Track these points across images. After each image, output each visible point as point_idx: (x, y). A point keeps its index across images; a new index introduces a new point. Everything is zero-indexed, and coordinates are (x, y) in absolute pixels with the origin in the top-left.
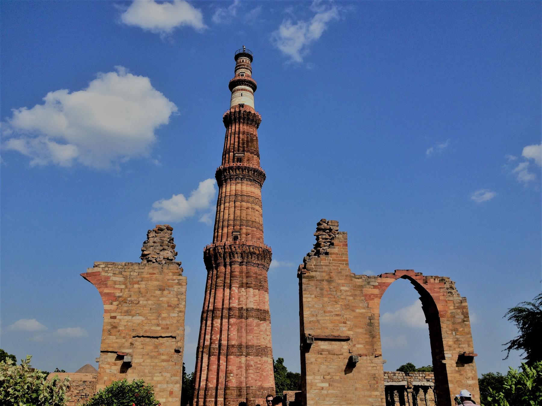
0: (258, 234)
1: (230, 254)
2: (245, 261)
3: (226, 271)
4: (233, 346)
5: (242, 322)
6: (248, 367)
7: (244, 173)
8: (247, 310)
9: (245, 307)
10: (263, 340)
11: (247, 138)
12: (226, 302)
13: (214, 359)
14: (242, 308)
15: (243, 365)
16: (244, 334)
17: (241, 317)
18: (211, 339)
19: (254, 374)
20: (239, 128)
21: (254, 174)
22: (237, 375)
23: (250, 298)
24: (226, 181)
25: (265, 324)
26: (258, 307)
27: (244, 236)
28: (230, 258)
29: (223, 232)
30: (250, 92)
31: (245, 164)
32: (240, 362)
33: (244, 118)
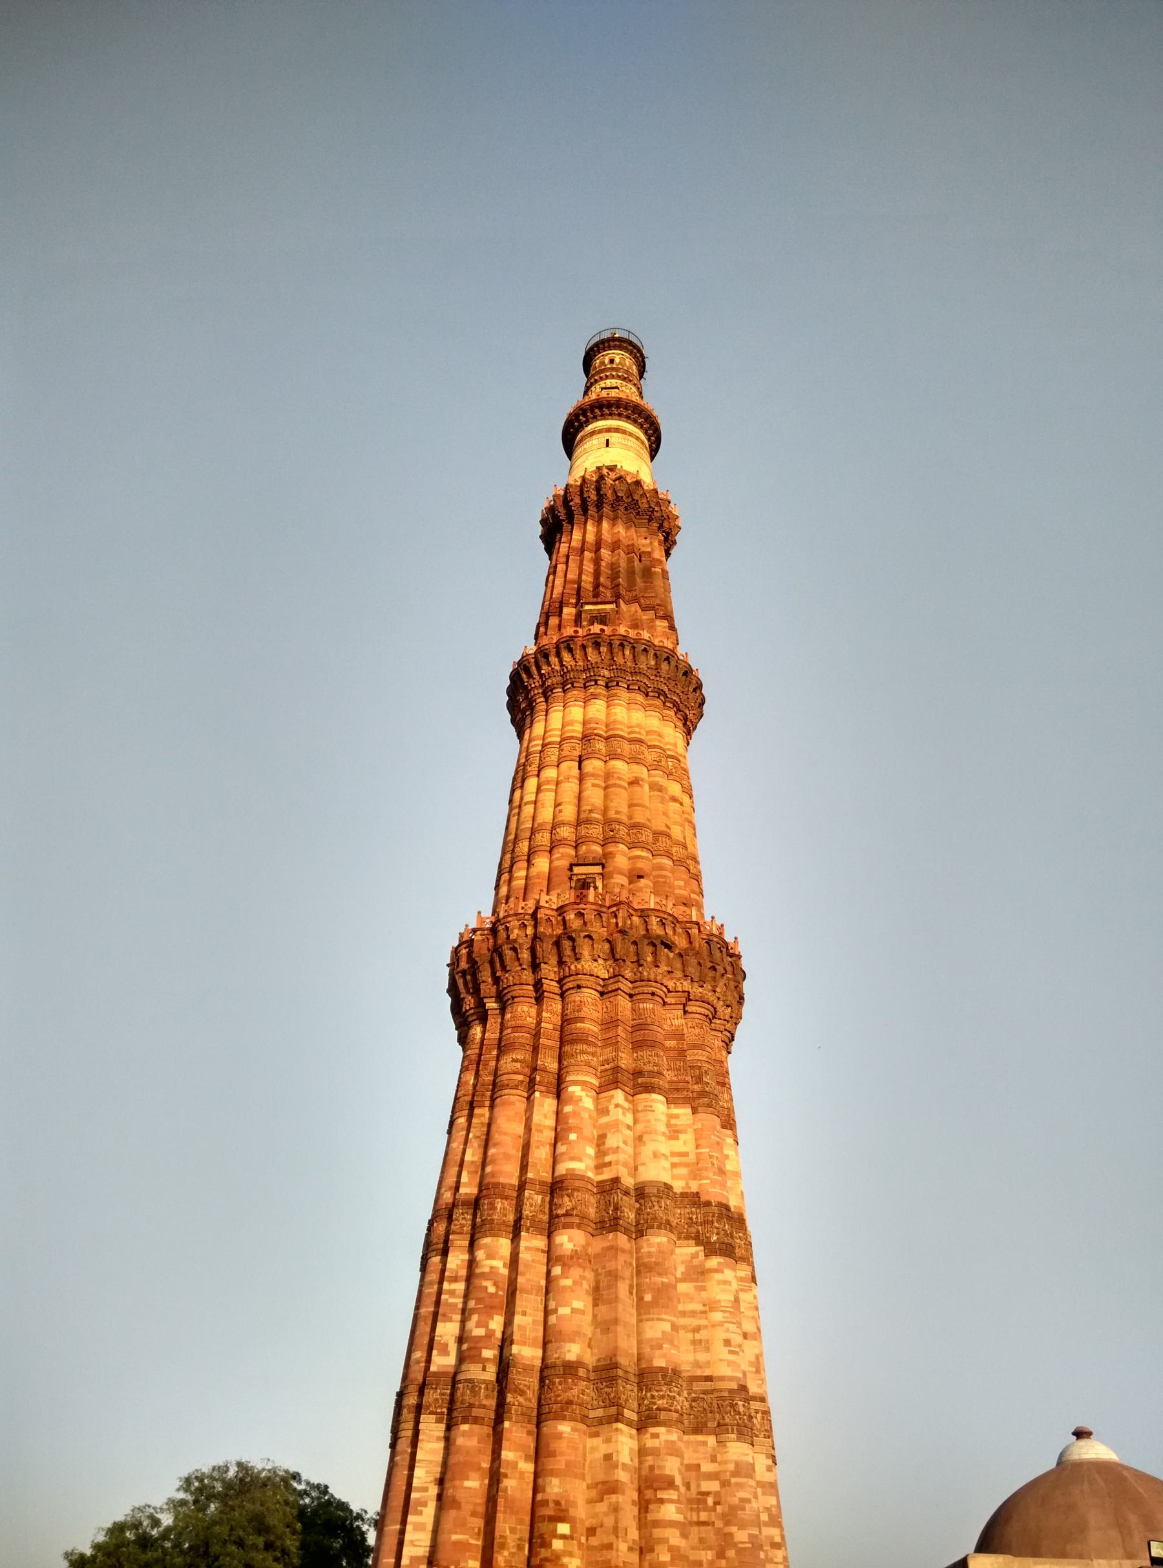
0: (680, 885)
1: (557, 944)
2: (628, 974)
3: (539, 1023)
4: (570, 1368)
5: (614, 1249)
6: (650, 1485)
7: (619, 659)
8: (641, 1193)
9: (628, 1181)
10: (723, 1353)
11: (630, 561)
12: (540, 1154)
13: (470, 1437)
14: (616, 1180)
15: (622, 1476)
16: (627, 1311)
17: (609, 1224)
18: (460, 1340)
19: (684, 1528)
20: (599, 534)
21: (657, 667)
22: (591, 1531)
23: (655, 1143)
24: (547, 693)
25: (728, 1274)
26: (694, 1187)
27: (624, 881)
28: (561, 963)
29: (534, 871)
30: (638, 438)
31: (622, 630)
32: (608, 1457)
33: (618, 499)
